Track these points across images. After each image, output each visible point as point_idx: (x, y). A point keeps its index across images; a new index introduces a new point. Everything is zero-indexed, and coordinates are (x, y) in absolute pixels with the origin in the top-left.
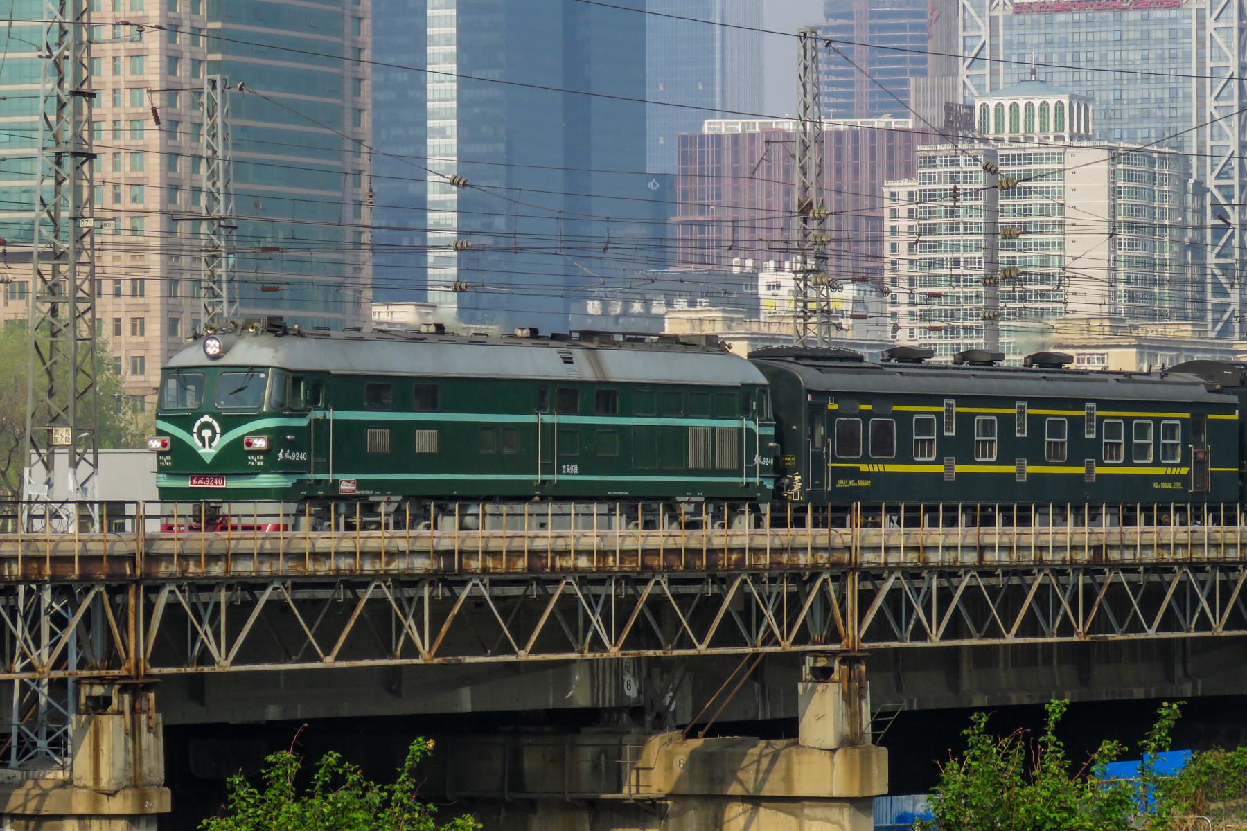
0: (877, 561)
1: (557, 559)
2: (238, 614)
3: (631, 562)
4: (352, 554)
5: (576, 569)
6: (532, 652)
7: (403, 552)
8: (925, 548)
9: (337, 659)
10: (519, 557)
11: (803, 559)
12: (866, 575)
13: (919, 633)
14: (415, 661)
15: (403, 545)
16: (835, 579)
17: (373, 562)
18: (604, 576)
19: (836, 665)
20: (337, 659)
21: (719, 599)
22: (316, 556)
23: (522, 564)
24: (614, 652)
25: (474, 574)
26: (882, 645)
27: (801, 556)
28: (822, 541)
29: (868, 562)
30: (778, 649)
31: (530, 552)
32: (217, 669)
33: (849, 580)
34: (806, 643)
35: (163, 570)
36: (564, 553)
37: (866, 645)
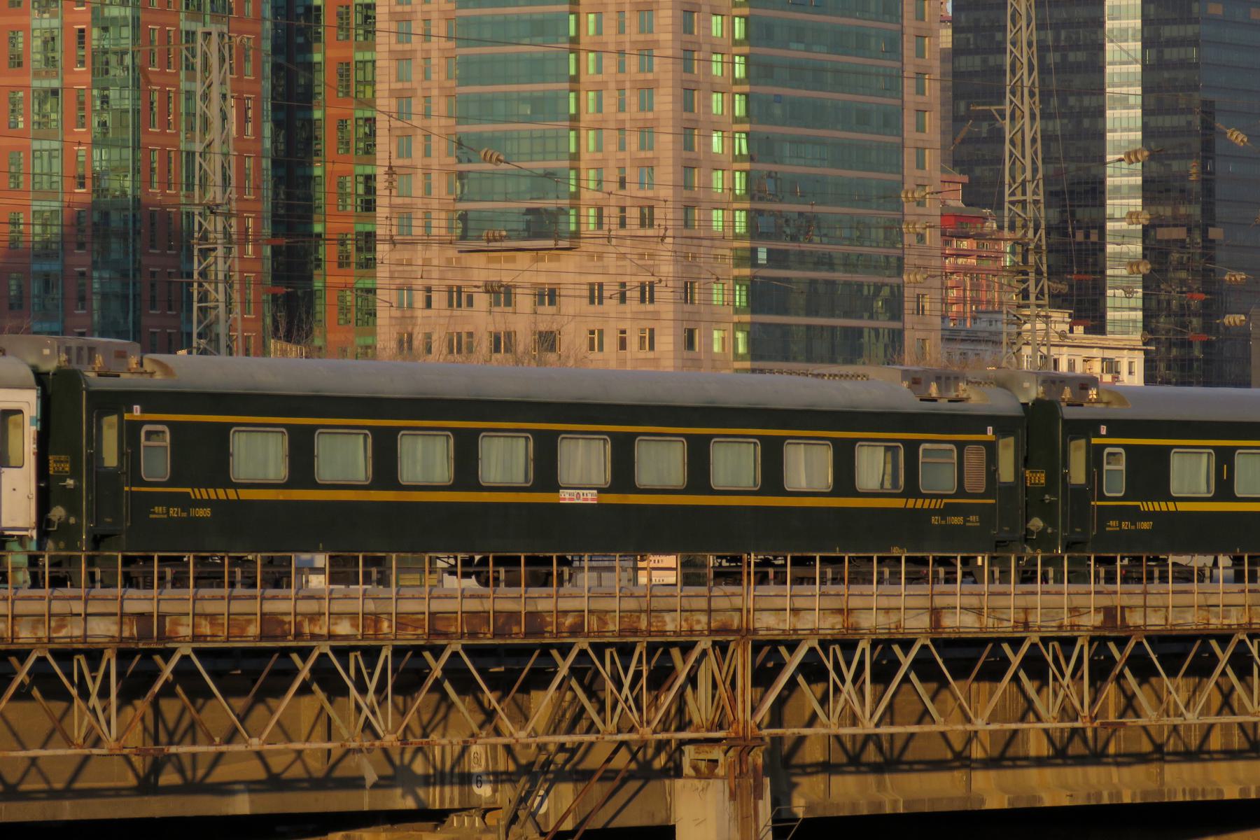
0: (782, 626)
1: (306, 624)
3: (416, 628)
5: (331, 636)
10: (249, 622)
17: (34, 628)
23: (253, 630)
25: (183, 640)
27: (668, 617)
29: (768, 629)
33: (740, 651)
36: (314, 617)
37: (765, 732)
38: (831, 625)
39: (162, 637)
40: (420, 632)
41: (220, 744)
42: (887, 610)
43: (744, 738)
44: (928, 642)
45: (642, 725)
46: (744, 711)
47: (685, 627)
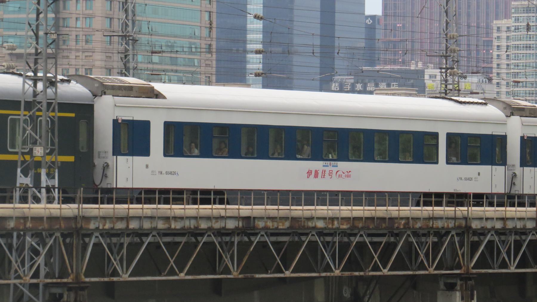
2: (133, 248)
4: (195, 218)
6: (293, 272)
7: (223, 217)
8: (507, 219)
9: (186, 274)
10: (286, 221)
11: (439, 224)
12: (475, 232)
13: (504, 265)
14: (229, 276)
15: (223, 213)
16: (457, 234)
18: (332, 231)
19: (459, 283)
20: (186, 274)
21: (395, 245)
22: (175, 218)
23: (287, 224)
24: (337, 273)
26: (483, 271)
28: (452, 214)
30: (427, 272)
31: (292, 218)
32: (121, 279)
34: (442, 269)
35: (92, 226)
36: (311, 219)
37: (474, 271)
38: (499, 225)
39: (254, 228)
40: (348, 226)
41: (271, 273)
42: (520, 219)
43: (467, 273)
44: (535, 233)
45: (429, 267)
46: (467, 261)
47: (446, 226)
